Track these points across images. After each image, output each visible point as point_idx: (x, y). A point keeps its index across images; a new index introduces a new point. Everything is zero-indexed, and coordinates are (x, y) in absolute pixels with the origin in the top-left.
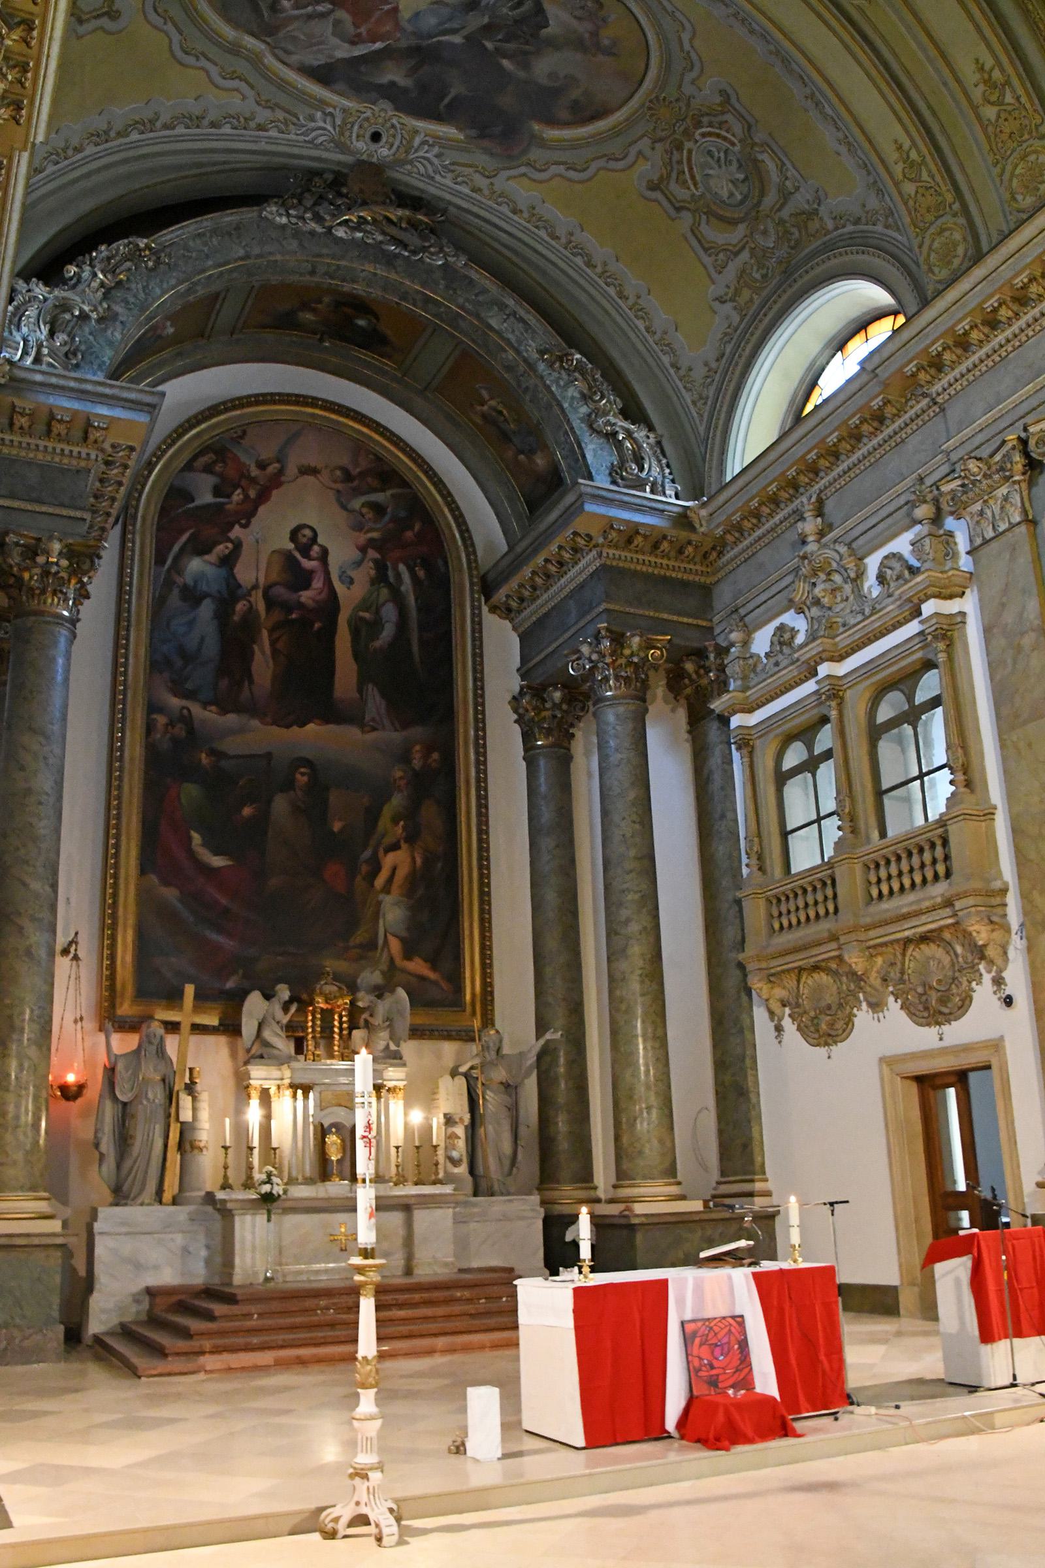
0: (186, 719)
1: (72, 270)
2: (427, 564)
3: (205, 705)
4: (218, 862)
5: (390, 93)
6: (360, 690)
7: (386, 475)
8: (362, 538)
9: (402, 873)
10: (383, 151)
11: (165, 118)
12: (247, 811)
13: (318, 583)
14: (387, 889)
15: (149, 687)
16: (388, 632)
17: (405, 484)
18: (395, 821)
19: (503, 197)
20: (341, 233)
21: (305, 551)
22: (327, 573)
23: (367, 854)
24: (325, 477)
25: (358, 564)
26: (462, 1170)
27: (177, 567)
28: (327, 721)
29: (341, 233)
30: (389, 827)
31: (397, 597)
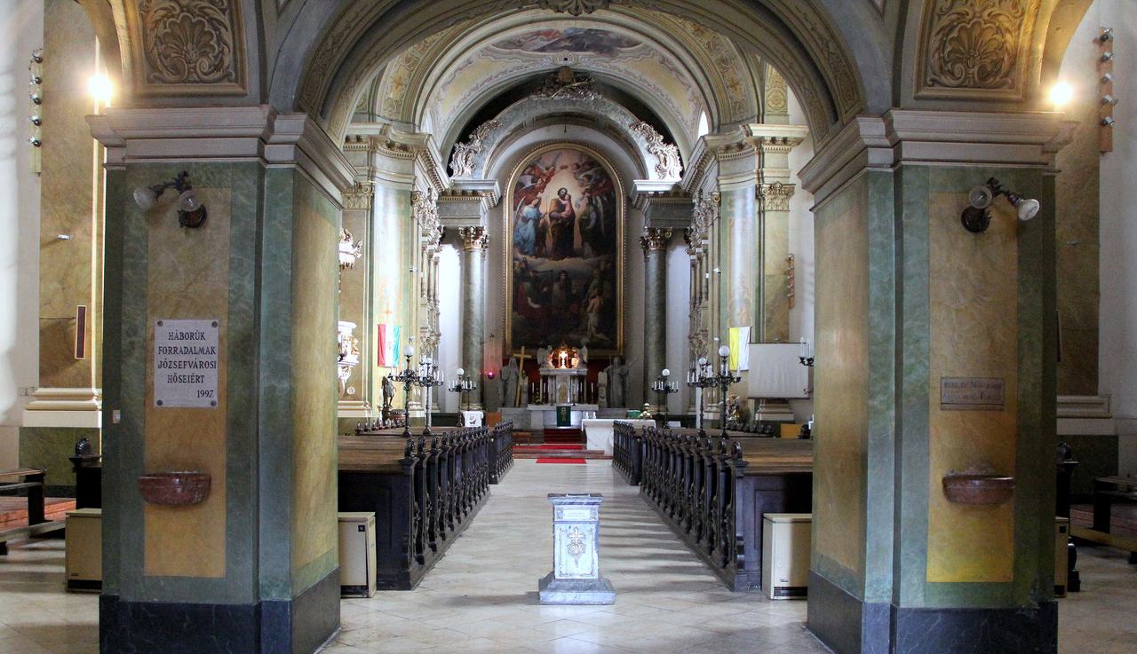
0: (525, 262)
1: (471, 136)
2: (608, 195)
3: (531, 256)
4: (536, 306)
5: (565, 48)
6: (582, 244)
7: (592, 163)
8: (583, 189)
9: (595, 307)
10: (569, 63)
11: (494, 75)
12: (545, 289)
13: (567, 209)
14: (591, 311)
15: (514, 253)
16: (593, 222)
17: (599, 165)
18: (594, 289)
19: (615, 68)
20: (556, 98)
21: (563, 198)
22: (571, 205)
23: (584, 300)
24: (570, 168)
25: (582, 199)
26: (605, 400)
27: (520, 211)
28: (571, 256)
29: (556, 98)
30: (592, 291)
31: (596, 209)
